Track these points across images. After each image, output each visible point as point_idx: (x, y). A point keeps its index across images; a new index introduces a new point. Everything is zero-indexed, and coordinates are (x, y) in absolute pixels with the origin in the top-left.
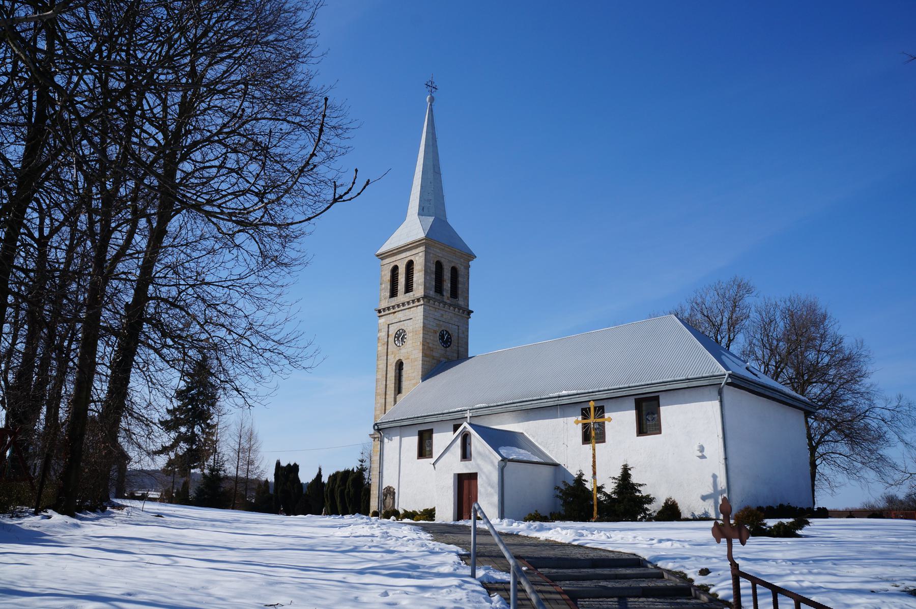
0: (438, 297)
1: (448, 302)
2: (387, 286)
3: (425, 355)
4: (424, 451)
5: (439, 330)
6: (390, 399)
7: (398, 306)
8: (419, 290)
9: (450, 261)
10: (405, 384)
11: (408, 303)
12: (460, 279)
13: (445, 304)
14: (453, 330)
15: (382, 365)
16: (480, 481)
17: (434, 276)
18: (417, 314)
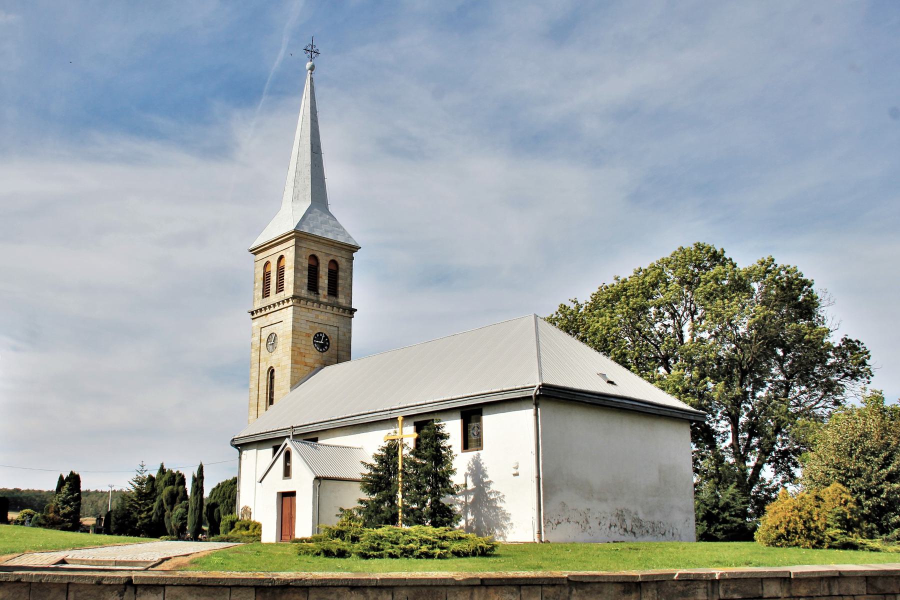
0: (312, 296)
1: (325, 300)
2: (260, 285)
3: (294, 362)
8: (289, 290)
9: (328, 255)
13: (320, 303)
15: (255, 374)
16: (298, 498)
17: (306, 273)
18: (287, 315)
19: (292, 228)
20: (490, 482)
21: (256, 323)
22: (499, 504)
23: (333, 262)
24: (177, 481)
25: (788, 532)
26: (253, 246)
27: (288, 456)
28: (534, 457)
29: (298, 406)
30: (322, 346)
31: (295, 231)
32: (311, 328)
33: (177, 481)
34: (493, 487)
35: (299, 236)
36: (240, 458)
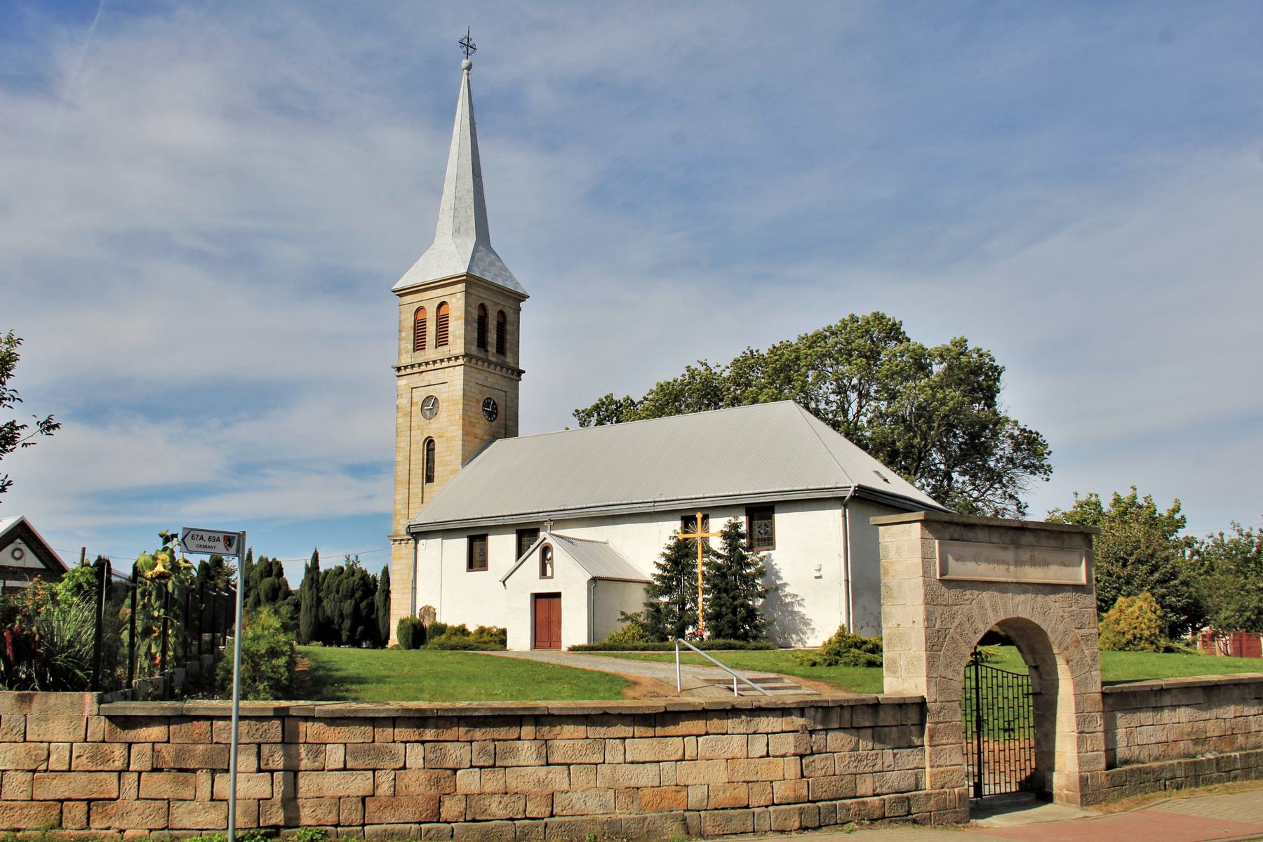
0: (482, 355)
1: (494, 359)
2: (409, 335)
4: (477, 560)
5: (482, 398)
6: (416, 490)
7: (427, 363)
9: (496, 304)
10: (438, 471)
11: (442, 361)
12: (508, 327)
13: (490, 363)
14: (498, 397)
15: (404, 444)
19: (464, 270)
20: (785, 584)
21: (402, 382)
22: (797, 609)
23: (501, 313)
24: (275, 572)
25: (1135, 638)
26: (398, 286)
27: (546, 549)
28: (842, 559)
29: (470, 488)
30: (490, 414)
31: (467, 275)
32: (481, 392)
33: (275, 572)
34: (788, 590)
35: (471, 281)
36: (416, 548)
